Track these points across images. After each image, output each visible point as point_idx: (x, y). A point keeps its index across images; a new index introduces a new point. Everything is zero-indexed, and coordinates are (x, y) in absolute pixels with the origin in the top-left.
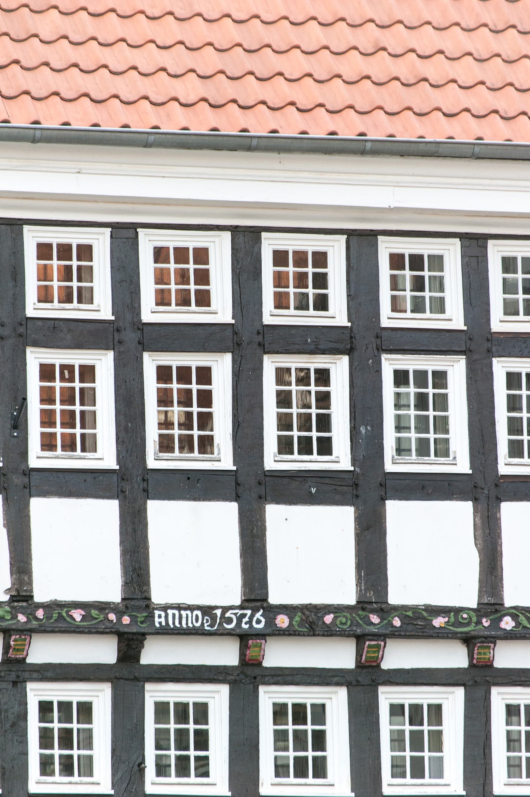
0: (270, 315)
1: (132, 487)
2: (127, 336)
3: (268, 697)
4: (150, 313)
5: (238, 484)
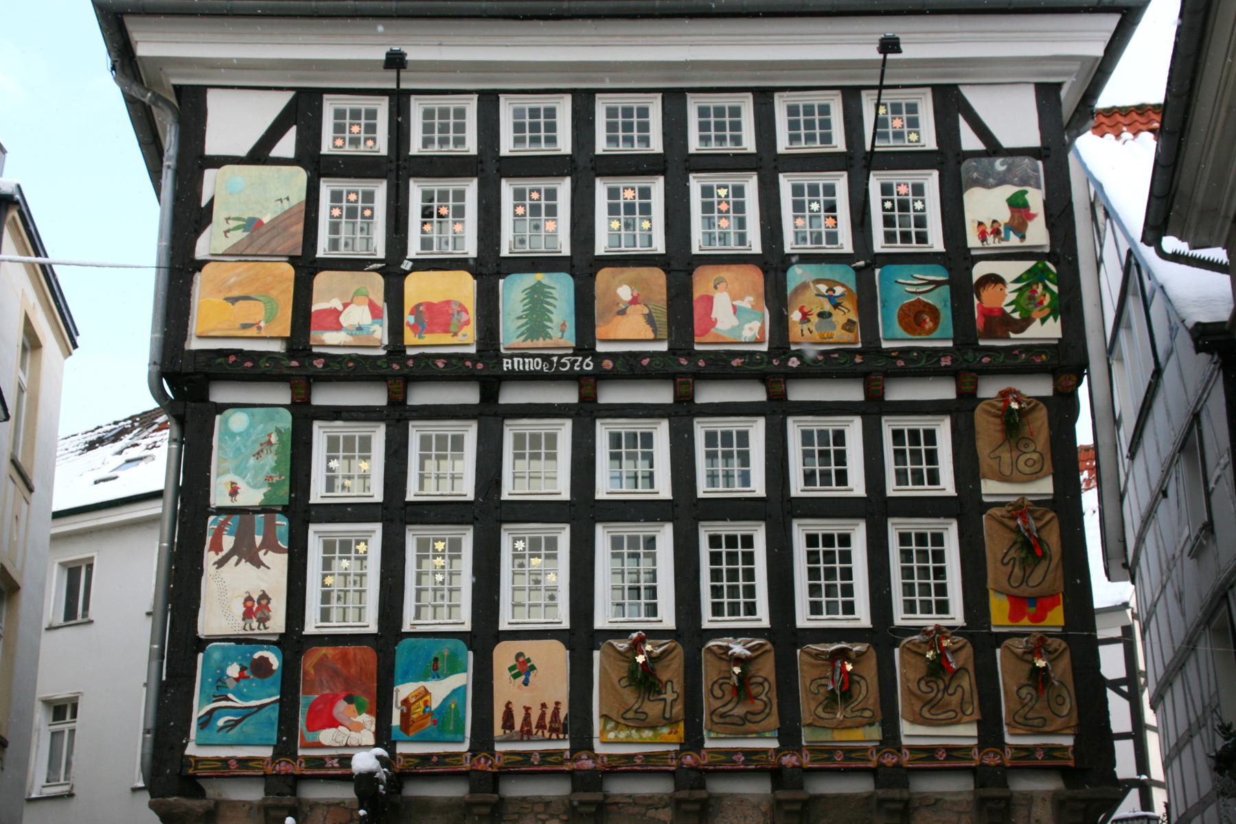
5: (573, 266)
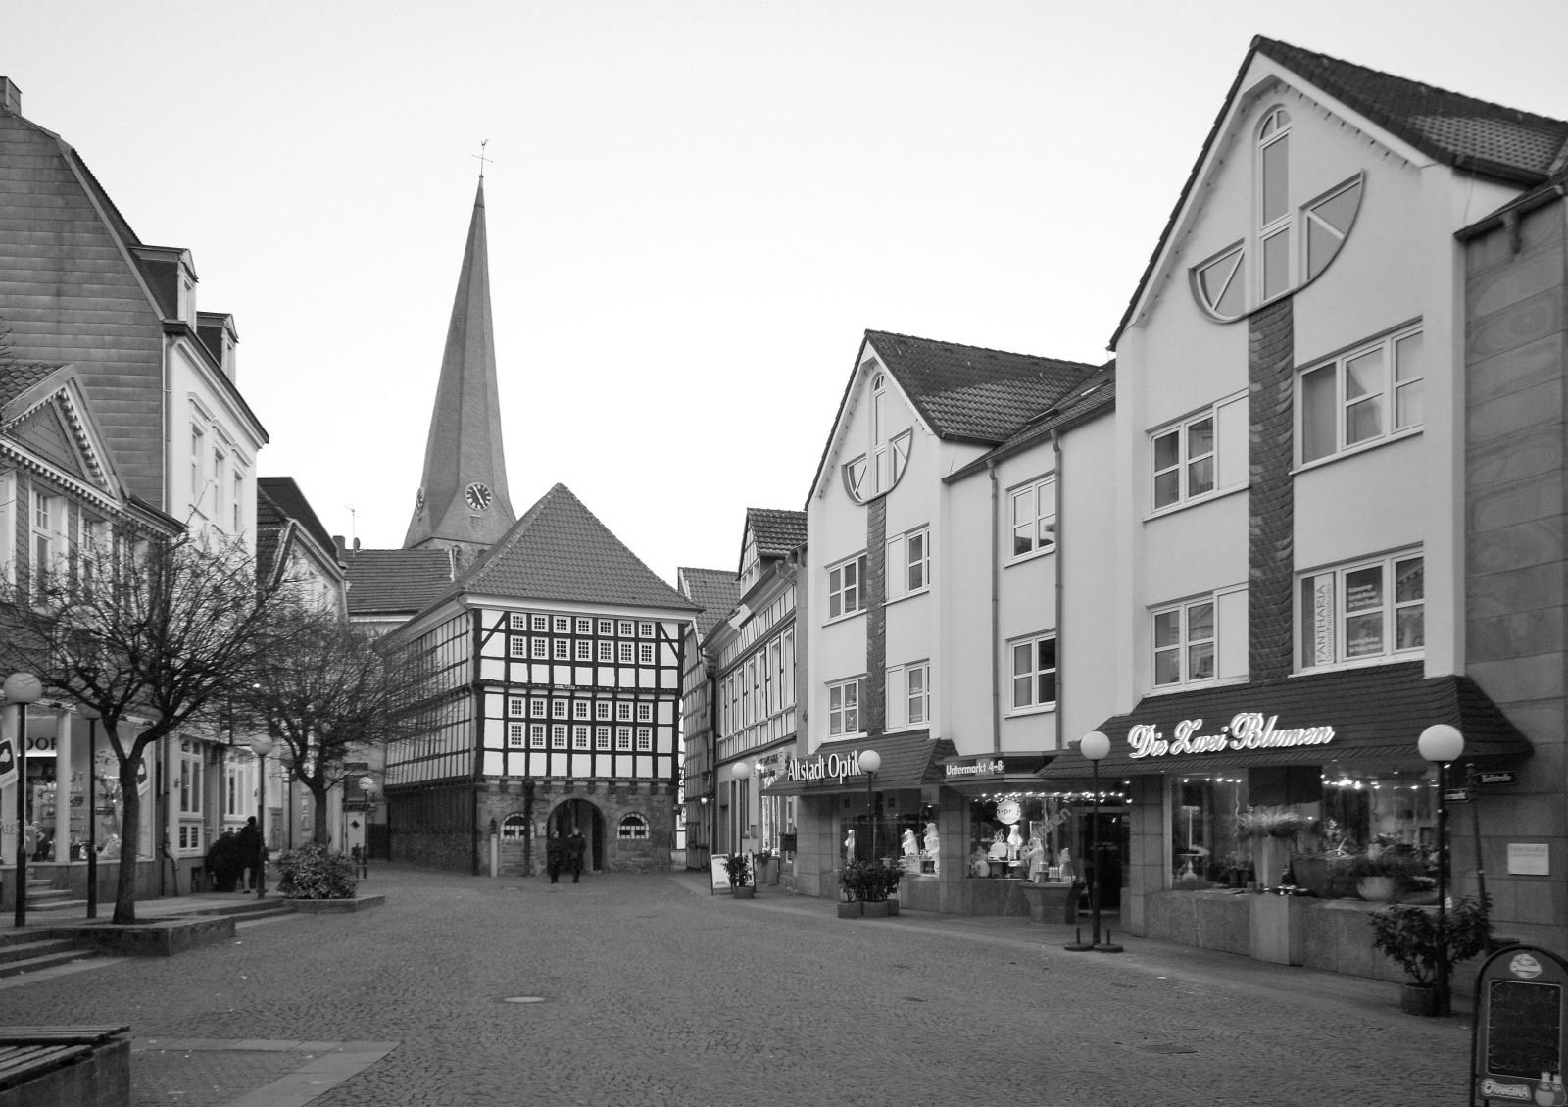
0: (578, 632)
1: (551, 663)
2: (551, 635)
3: (575, 702)
4: (555, 631)
